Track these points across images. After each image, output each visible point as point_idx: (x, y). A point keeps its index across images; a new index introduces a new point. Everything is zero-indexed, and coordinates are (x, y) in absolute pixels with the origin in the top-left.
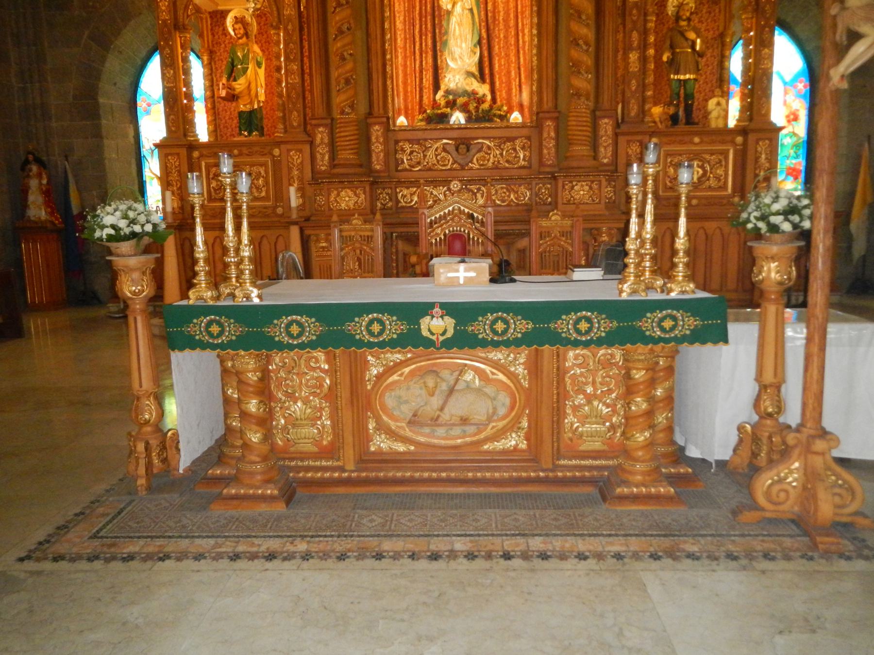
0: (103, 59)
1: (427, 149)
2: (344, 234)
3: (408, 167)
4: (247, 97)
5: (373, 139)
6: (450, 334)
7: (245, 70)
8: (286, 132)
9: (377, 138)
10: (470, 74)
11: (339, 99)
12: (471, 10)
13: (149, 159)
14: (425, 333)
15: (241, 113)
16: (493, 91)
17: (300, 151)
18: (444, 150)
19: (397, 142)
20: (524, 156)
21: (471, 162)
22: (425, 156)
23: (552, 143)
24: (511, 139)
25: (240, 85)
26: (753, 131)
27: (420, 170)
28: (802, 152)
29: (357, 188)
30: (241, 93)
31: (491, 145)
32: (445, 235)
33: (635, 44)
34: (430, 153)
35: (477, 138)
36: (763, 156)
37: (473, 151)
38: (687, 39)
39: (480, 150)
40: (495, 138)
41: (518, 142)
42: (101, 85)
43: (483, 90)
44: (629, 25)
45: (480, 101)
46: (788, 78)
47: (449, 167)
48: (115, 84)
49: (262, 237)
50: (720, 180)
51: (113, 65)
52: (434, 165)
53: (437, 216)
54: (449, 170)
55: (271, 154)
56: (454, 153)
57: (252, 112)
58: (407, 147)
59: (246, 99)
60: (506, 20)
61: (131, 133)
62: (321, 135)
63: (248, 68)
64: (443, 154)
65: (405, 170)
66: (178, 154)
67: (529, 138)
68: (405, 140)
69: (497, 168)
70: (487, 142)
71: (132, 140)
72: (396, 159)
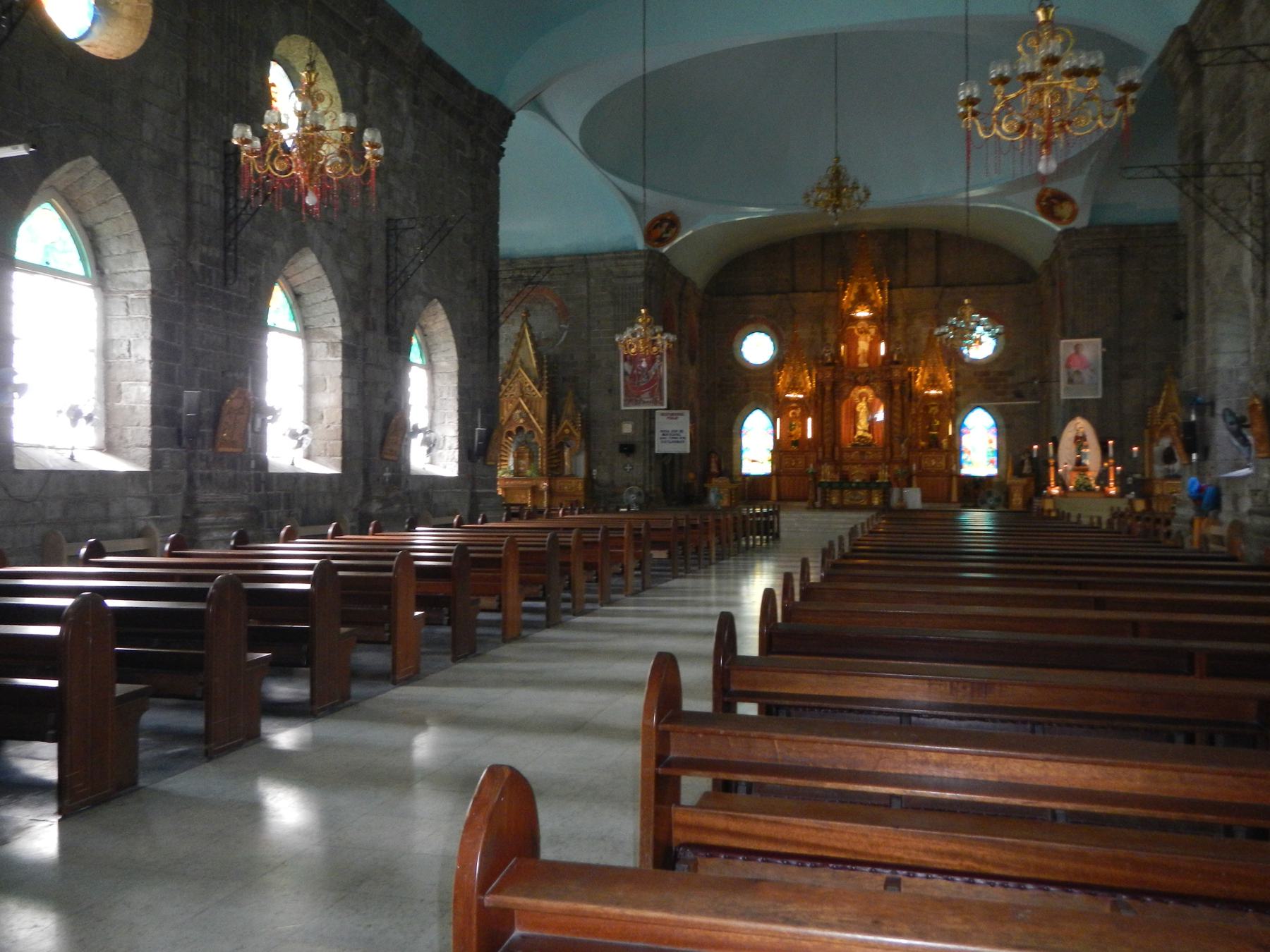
10: (865, 431)
11: (826, 440)
16: (873, 435)
25: (793, 432)
28: (995, 453)
43: (869, 435)
45: (868, 439)
51: (738, 419)
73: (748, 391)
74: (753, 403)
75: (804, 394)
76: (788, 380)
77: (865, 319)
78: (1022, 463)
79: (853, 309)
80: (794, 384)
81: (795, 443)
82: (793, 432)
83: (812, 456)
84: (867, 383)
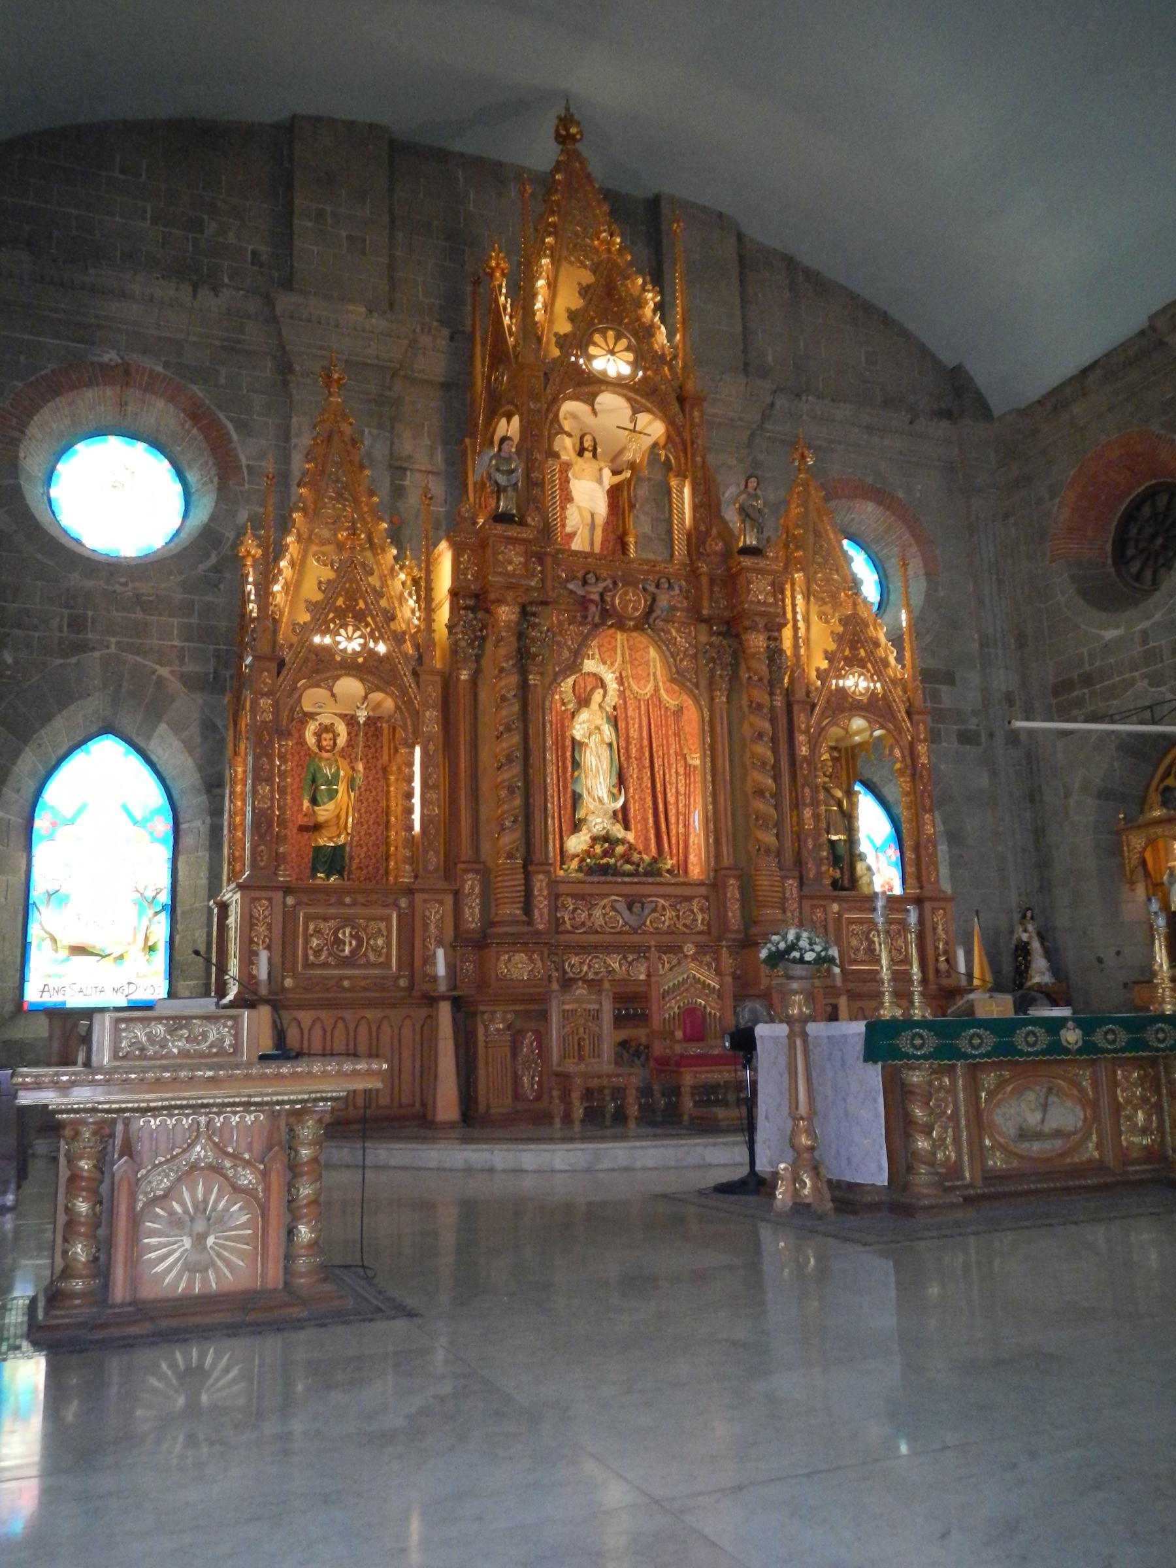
0: (16, 755)
1: (592, 907)
2: (567, 1007)
3: (570, 928)
4: (334, 828)
5: (536, 893)
6: (1080, 1043)
7: (332, 794)
8: (416, 877)
9: (541, 890)
12: (610, 745)
13: (42, 909)
14: (1065, 1044)
15: (318, 849)
17: (441, 902)
18: (614, 909)
19: (557, 896)
20: (703, 920)
21: (644, 924)
22: (590, 915)
23: (737, 906)
24: (688, 899)
25: (325, 812)
26: (931, 899)
27: (585, 933)
29: (534, 952)
30: (326, 822)
31: (666, 904)
32: (679, 1007)
33: (808, 801)
34: (598, 913)
35: (650, 896)
36: (940, 927)
37: (647, 911)
38: (833, 797)
39: (654, 910)
40: (670, 896)
41: (695, 902)
42: (5, 790)
44: (800, 781)
46: (878, 843)
47: (618, 930)
48: (19, 790)
49: (381, 1022)
50: (901, 953)
51: (27, 762)
52: (601, 926)
53: (671, 984)
54: (619, 933)
55: (396, 905)
56: (626, 913)
57: (339, 849)
58: (570, 903)
59: (333, 831)
60: (640, 759)
61: (24, 867)
62: (471, 884)
63: (337, 791)
64: (613, 913)
65: (569, 932)
66: (270, 900)
67: (706, 898)
68: (568, 895)
69: (673, 933)
70: (662, 901)
71: (23, 876)
72: (557, 919)
73: (82, 648)
74: (95, 703)
75: (397, 639)
76: (319, 572)
77: (618, 385)
78: (1023, 950)
79: (579, 340)
80: (352, 597)
81: (333, 861)
82: (325, 812)
83: (436, 913)
84: (646, 622)
